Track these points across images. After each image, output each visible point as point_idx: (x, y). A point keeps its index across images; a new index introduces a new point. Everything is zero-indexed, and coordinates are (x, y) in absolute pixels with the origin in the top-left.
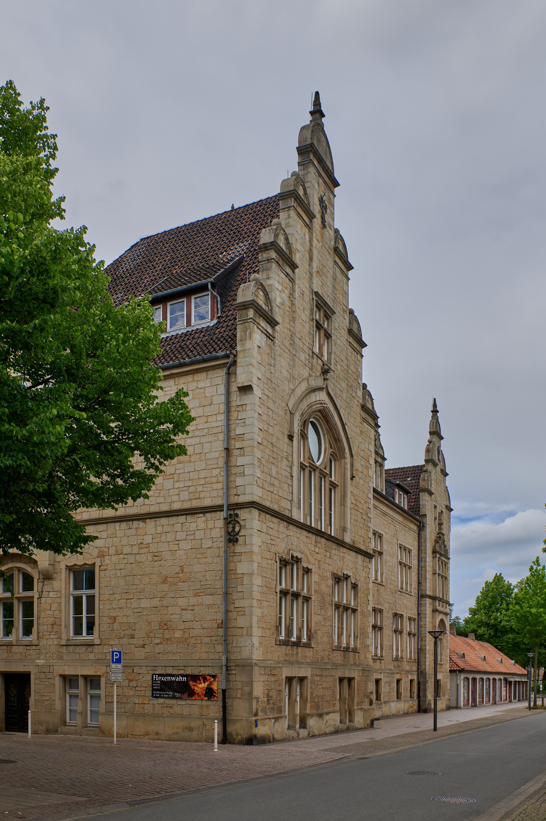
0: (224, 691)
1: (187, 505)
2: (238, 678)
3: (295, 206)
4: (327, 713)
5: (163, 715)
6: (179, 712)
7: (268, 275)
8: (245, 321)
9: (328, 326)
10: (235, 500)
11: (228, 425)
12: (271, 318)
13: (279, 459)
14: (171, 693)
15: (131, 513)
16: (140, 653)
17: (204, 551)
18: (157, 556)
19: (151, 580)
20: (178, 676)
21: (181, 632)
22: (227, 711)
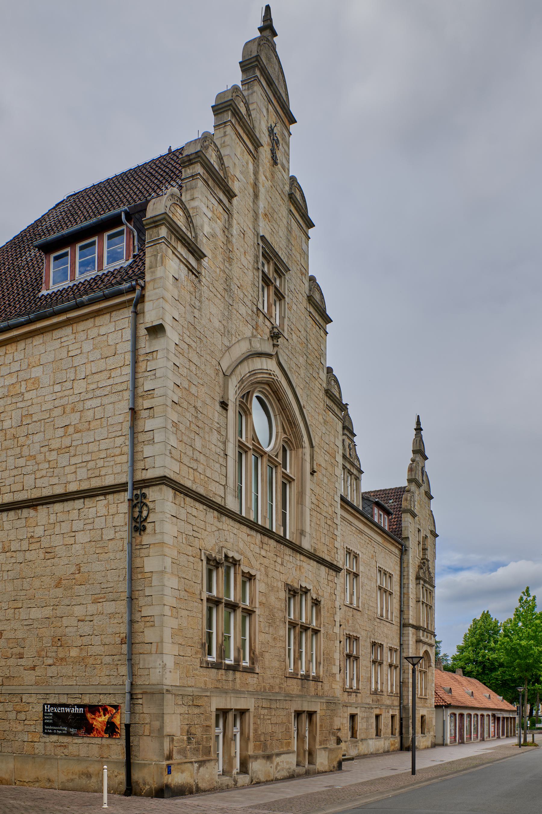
0: (128, 726)
1: (85, 486)
2: (146, 708)
3: (233, 121)
4: (278, 755)
5: (56, 757)
6: (75, 753)
7: (193, 195)
8: (156, 242)
9: (280, 284)
10: (141, 475)
11: (135, 379)
12: (193, 246)
13: (207, 429)
14: (66, 729)
15: (20, 499)
16: (30, 677)
17: (105, 545)
18: (49, 552)
19: (42, 584)
20: (73, 706)
21: (77, 650)
22: (132, 753)
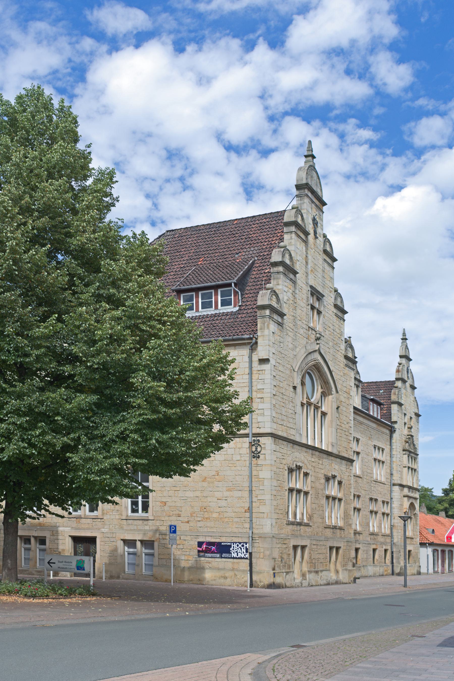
4: (322, 571)
